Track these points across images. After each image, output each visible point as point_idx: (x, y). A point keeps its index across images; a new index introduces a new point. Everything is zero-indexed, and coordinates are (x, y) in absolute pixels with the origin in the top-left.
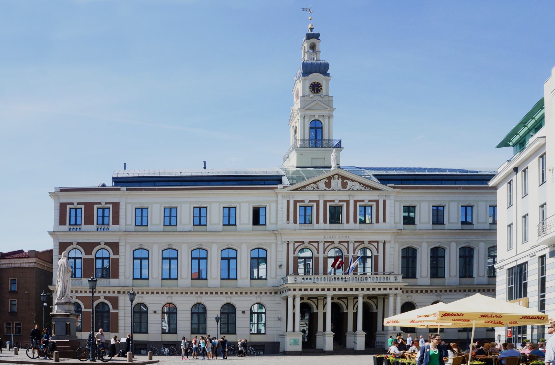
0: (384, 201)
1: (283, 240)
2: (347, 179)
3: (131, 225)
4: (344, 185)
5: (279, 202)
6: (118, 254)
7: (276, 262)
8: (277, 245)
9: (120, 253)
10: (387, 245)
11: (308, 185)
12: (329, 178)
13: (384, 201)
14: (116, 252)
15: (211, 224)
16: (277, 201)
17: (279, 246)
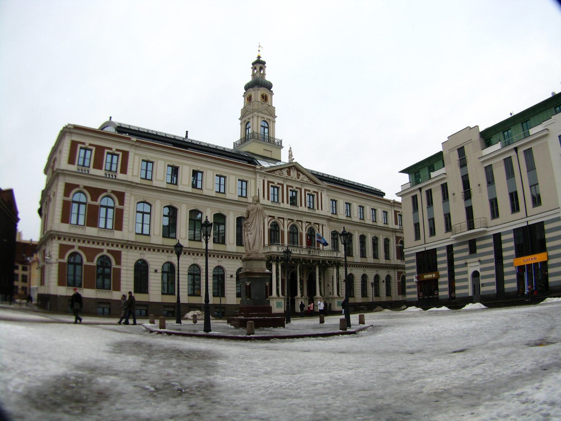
0: (321, 194)
2: (300, 171)
3: (137, 176)
4: (298, 176)
5: (258, 180)
10: (324, 227)
11: (276, 170)
12: (289, 168)
13: (321, 194)
14: (122, 202)
15: (206, 189)
16: (256, 179)
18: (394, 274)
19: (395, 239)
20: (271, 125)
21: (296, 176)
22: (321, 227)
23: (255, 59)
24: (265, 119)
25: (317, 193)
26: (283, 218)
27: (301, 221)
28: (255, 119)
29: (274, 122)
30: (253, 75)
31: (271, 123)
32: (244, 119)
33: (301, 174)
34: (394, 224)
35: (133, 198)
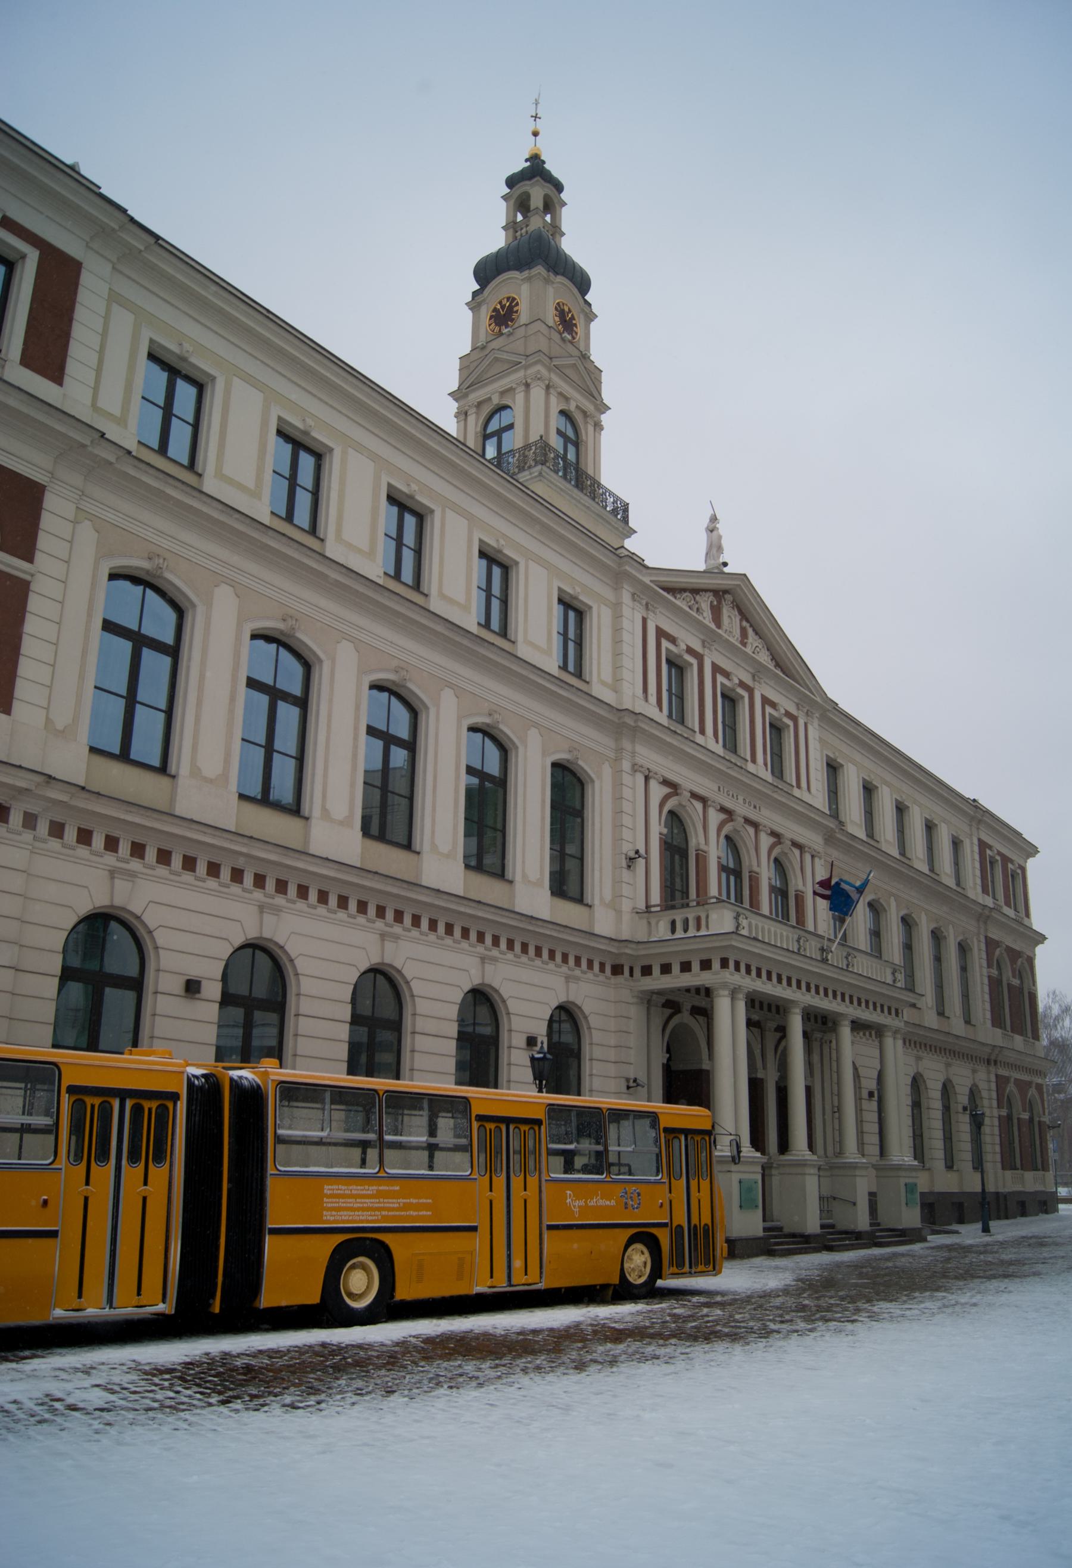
1: (639, 760)
2: (748, 621)
5: (626, 611)
6: (30, 559)
7: (617, 840)
8: (618, 773)
9: (39, 556)
10: (817, 860)
17: (627, 779)
18: (985, 1080)
19: (983, 946)
20: (587, 432)
21: (737, 632)
22: (808, 858)
23: (520, 164)
24: (572, 407)
25: (795, 719)
26: (703, 800)
27: (755, 825)
28: (537, 392)
29: (598, 426)
30: (511, 226)
31: (591, 428)
32: (476, 396)
33: (750, 631)
34: (979, 889)
35: (87, 534)
